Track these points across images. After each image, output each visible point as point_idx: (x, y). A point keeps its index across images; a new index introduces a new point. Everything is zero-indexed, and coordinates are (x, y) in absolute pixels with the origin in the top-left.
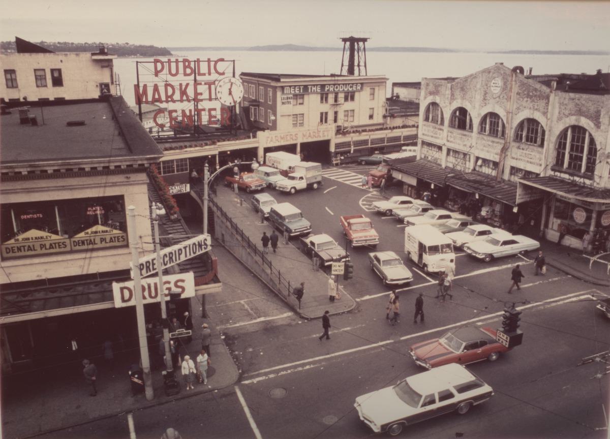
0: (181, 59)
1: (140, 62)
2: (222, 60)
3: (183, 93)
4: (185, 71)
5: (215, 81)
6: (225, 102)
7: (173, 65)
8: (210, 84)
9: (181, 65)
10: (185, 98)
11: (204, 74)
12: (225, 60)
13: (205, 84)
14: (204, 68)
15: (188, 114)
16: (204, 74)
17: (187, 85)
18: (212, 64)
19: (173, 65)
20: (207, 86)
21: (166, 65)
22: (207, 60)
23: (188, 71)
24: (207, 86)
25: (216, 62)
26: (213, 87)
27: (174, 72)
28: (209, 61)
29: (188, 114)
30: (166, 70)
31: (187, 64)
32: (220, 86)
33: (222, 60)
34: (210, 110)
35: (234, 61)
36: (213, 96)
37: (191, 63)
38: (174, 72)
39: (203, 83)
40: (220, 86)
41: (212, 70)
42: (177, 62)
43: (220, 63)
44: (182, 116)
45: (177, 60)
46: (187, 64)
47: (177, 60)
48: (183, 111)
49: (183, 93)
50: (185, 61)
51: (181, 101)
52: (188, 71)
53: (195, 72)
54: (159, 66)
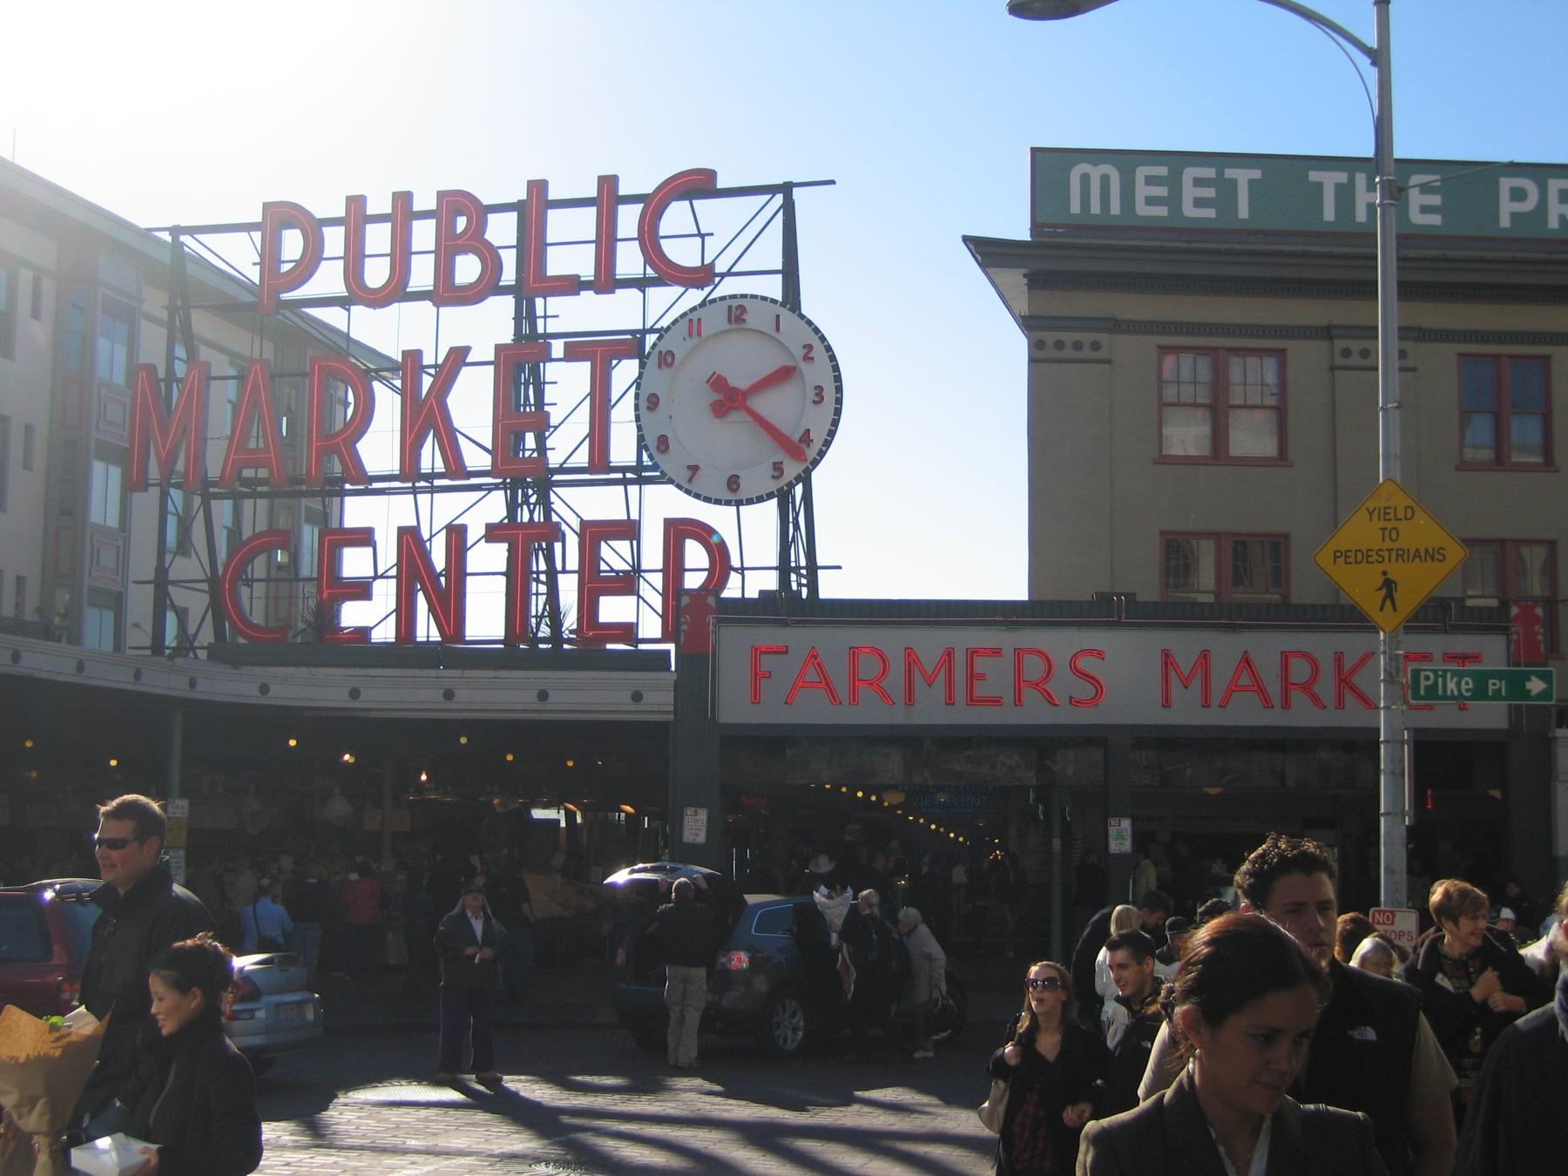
0: (425, 201)
1: (193, 231)
2: (697, 185)
3: (426, 417)
4: (444, 269)
5: (644, 332)
6: (694, 469)
7: (378, 238)
8: (598, 351)
9: (424, 234)
10: (430, 457)
11: (571, 285)
12: (720, 185)
13: (572, 354)
14: (570, 245)
15: (439, 561)
16: (571, 285)
17: (458, 357)
18: (628, 219)
19: (378, 238)
20: (584, 369)
21: (334, 240)
22: (592, 192)
23: (467, 269)
24: (584, 369)
25: (653, 206)
26: (625, 372)
27: (377, 274)
28: (608, 197)
29: (439, 561)
30: (329, 279)
31: (461, 223)
32: (666, 359)
33: (697, 185)
34: (595, 533)
35: (786, 189)
36: (623, 449)
37: (492, 218)
38: (377, 274)
39: (558, 348)
40: (666, 359)
41: (629, 261)
42: (403, 212)
43: (676, 217)
44: (398, 577)
45: (403, 200)
46: (461, 223)
47: (403, 200)
48: (410, 539)
49: (426, 417)
50: (455, 203)
51: (410, 476)
52: (467, 269)
53: (534, 283)
54: (292, 244)
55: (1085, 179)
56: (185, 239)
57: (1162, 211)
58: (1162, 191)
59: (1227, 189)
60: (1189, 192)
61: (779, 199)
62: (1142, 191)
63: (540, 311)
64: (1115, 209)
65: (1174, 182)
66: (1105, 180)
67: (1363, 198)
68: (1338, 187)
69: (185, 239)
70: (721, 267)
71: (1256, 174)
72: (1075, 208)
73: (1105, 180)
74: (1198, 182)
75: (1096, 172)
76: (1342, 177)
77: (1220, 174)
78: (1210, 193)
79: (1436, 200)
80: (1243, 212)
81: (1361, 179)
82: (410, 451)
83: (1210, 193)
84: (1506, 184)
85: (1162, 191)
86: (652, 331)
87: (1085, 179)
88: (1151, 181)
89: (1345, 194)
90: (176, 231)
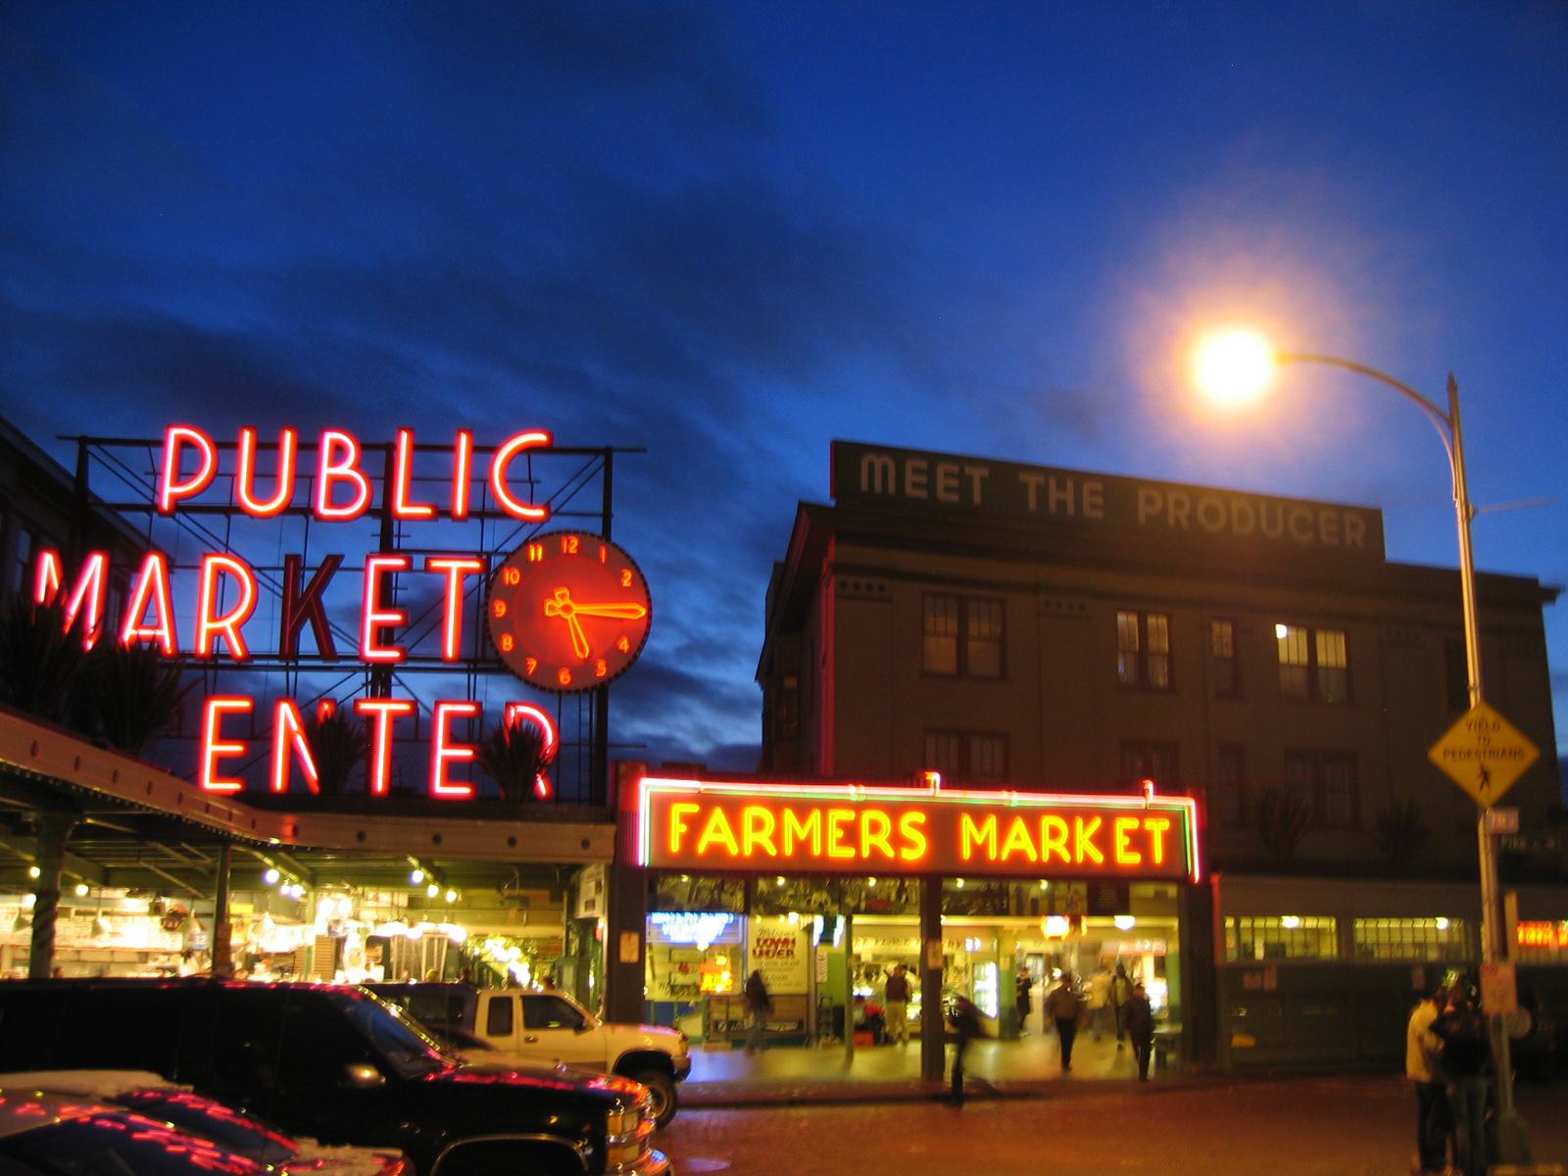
1: (98, 442)
10: (308, 642)
35: (607, 453)
55: (871, 466)
56: (91, 448)
57: (923, 494)
58: (923, 479)
59: (966, 482)
60: (941, 481)
61: (601, 459)
62: (910, 478)
63: (395, 531)
64: (892, 489)
65: (931, 473)
66: (885, 468)
67: (1054, 495)
68: (1039, 487)
69: (91, 448)
70: (553, 509)
71: (985, 472)
72: (864, 485)
73: (885, 468)
74: (947, 475)
75: (878, 462)
76: (1041, 479)
77: (962, 470)
78: (955, 483)
79: (1099, 500)
80: (977, 498)
81: (1052, 483)
82: (289, 638)
83: (955, 483)
84: (1142, 494)
85: (923, 479)
86: (496, 552)
87: (871, 466)
88: (916, 471)
89: (1042, 491)
90: (84, 442)
